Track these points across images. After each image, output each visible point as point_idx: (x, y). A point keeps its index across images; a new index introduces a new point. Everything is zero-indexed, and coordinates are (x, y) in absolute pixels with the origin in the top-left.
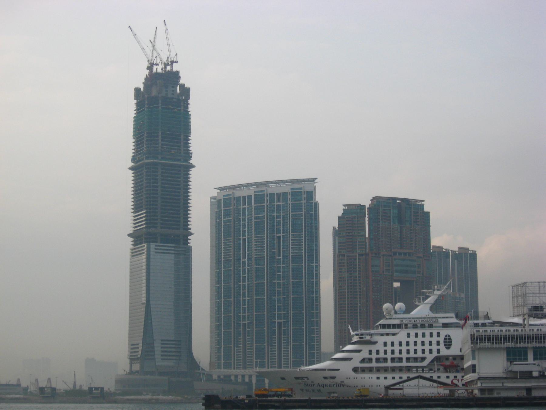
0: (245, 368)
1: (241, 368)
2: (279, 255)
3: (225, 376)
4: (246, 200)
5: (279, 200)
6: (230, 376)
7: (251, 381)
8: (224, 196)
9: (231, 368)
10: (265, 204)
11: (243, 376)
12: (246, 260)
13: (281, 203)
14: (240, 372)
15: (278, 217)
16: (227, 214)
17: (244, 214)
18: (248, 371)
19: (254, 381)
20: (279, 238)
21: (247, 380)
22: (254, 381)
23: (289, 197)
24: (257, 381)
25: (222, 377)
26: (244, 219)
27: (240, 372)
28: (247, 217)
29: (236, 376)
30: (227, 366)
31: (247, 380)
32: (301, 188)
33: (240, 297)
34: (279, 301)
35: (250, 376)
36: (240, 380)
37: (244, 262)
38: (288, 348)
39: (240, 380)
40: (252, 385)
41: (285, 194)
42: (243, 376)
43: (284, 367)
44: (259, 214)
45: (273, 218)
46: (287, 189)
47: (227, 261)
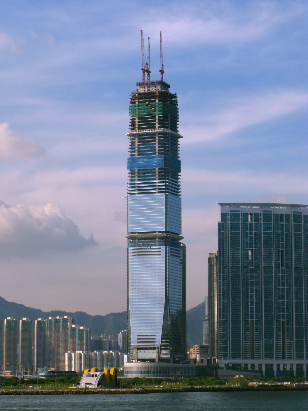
0: (253, 358)
1: (249, 358)
2: (282, 266)
3: (233, 365)
4: (279, 217)
5: (282, 221)
6: (239, 365)
8: (231, 211)
9: (241, 358)
10: (272, 222)
11: (253, 365)
12: (253, 267)
13: (284, 223)
15: (282, 234)
16: (234, 226)
17: (251, 229)
18: (256, 362)
19: (264, 368)
20: (282, 251)
21: (257, 368)
22: (264, 368)
23: (292, 218)
24: (266, 369)
25: (230, 365)
26: (251, 233)
27: (249, 362)
28: (254, 231)
29: (246, 365)
30: (236, 356)
31: (257, 368)
32: (301, 213)
33: (248, 299)
34: (283, 303)
35: (260, 365)
36: (249, 368)
37: (251, 270)
38: (260, 343)
40: (293, 371)
41: (288, 216)
42: (253, 365)
43: (287, 358)
44: (267, 230)
45: (278, 234)
46: (290, 212)
47: (235, 267)
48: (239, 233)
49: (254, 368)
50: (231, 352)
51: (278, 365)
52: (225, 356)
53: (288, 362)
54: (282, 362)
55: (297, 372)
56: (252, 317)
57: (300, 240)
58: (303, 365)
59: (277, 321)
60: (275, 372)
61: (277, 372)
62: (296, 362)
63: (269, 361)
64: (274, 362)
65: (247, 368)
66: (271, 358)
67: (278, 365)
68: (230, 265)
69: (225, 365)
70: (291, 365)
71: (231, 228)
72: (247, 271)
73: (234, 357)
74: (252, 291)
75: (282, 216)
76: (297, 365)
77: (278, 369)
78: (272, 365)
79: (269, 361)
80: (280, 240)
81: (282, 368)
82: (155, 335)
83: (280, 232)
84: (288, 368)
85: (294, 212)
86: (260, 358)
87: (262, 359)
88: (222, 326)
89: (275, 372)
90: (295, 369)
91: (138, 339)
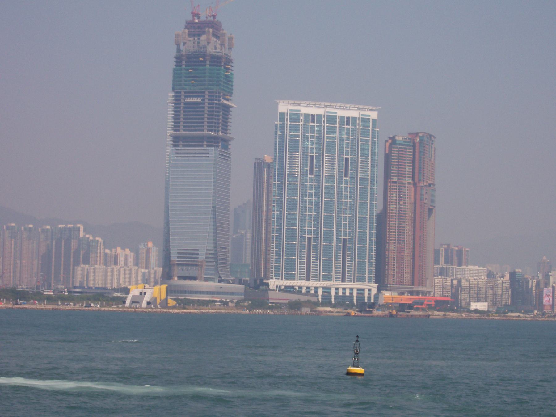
0: (308, 279)
3: (286, 287)
5: (348, 124)
6: (293, 287)
7: (316, 292)
14: (304, 283)
18: (312, 284)
21: (312, 292)
25: (283, 287)
27: (304, 283)
29: (300, 287)
32: (369, 116)
33: (306, 212)
35: (316, 289)
36: (304, 290)
39: (304, 290)
48: (298, 136)
49: (309, 292)
50: (284, 272)
51: (337, 289)
52: (277, 276)
53: (348, 285)
54: (340, 284)
55: (357, 297)
56: (310, 232)
57: (366, 148)
58: (363, 290)
59: (338, 239)
60: (333, 298)
61: (335, 296)
62: (357, 285)
63: (326, 284)
64: (332, 284)
65: (301, 291)
66: (329, 280)
67: (337, 289)
68: (287, 173)
69: (277, 287)
70: (351, 289)
71: (290, 130)
72: (307, 179)
73: (287, 278)
74: (311, 203)
75: (348, 118)
76: (358, 289)
77: (336, 293)
78: (330, 288)
79: (326, 284)
80: (345, 146)
81: (340, 293)
82: (198, 250)
83: (345, 137)
84: (348, 293)
85: (362, 115)
86: (317, 280)
87: (319, 281)
88: (275, 242)
89: (333, 298)
90: (355, 294)
91: (179, 253)
